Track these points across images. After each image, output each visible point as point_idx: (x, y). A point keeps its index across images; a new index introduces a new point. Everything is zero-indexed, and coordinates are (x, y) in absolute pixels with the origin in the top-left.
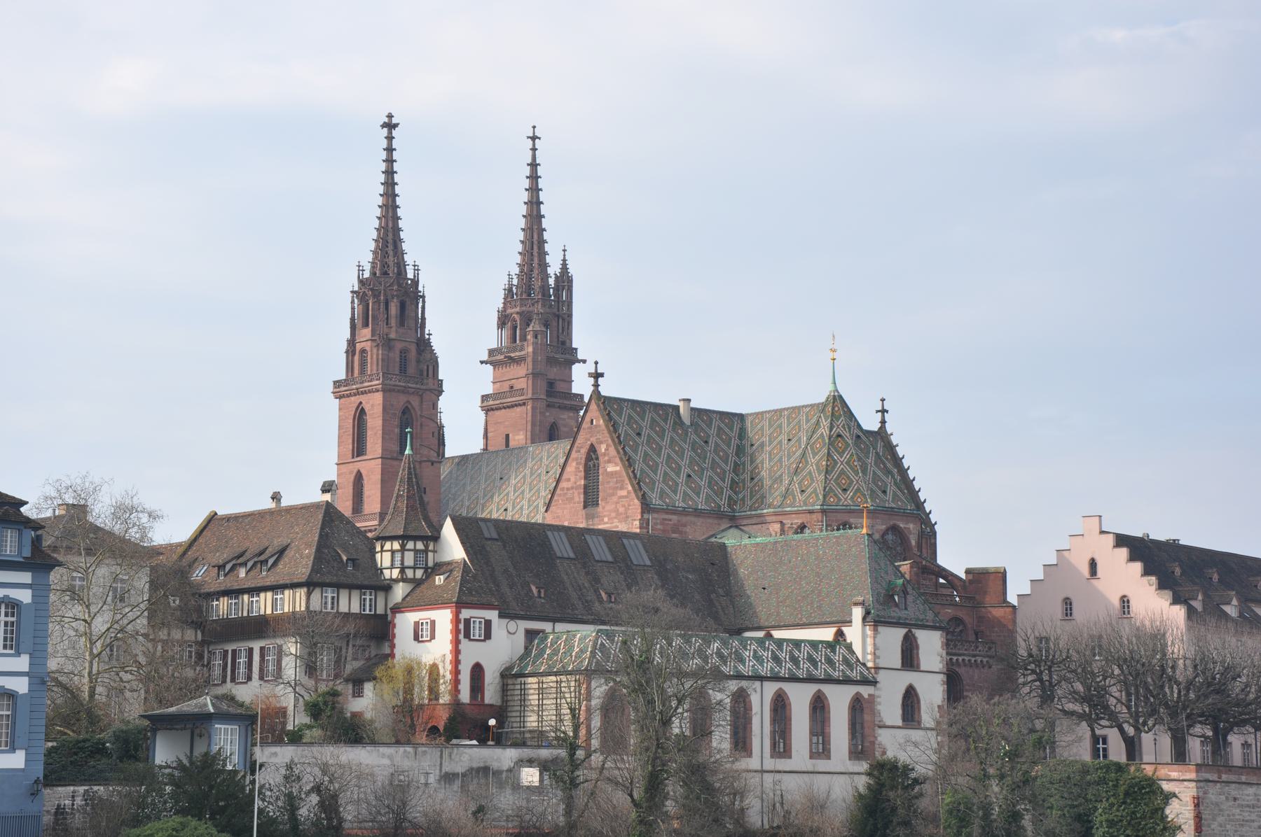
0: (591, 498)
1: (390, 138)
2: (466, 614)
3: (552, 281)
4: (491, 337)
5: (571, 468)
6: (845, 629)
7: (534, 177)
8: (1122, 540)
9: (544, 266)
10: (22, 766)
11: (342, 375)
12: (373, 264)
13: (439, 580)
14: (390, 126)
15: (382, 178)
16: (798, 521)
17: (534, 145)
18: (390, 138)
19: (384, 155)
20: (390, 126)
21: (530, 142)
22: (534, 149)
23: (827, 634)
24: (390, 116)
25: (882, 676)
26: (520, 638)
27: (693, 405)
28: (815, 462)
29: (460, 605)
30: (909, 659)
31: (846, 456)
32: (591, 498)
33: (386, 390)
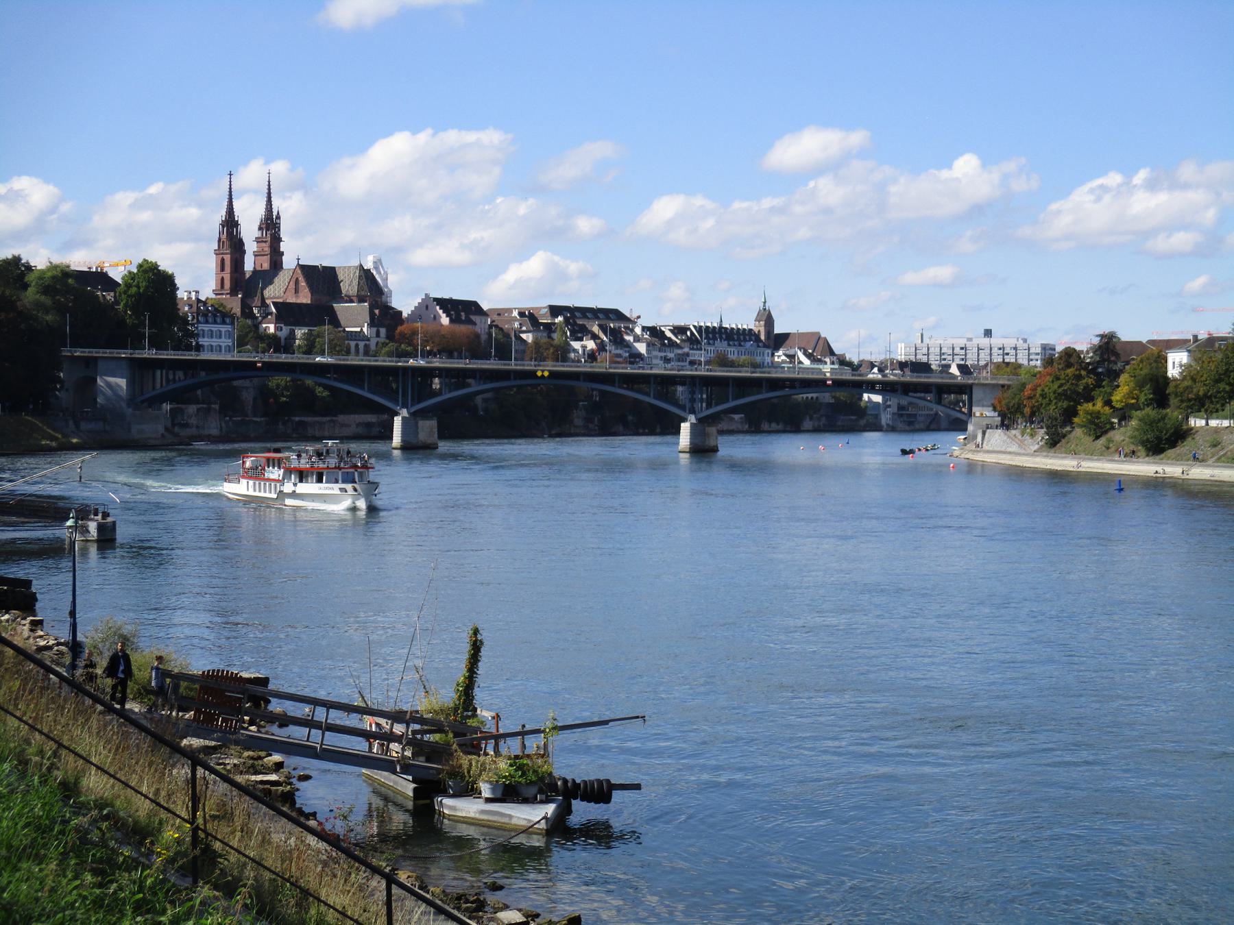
0: (297, 291)
4: (257, 234)
7: (269, 185)
11: (217, 248)
13: (269, 317)
14: (230, 175)
20: (230, 175)
23: (358, 329)
25: (372, 339)
28: (355, 283)
29: (275, 324)
30: (378, 335)
32: (297, 291)
33: (231, 254)
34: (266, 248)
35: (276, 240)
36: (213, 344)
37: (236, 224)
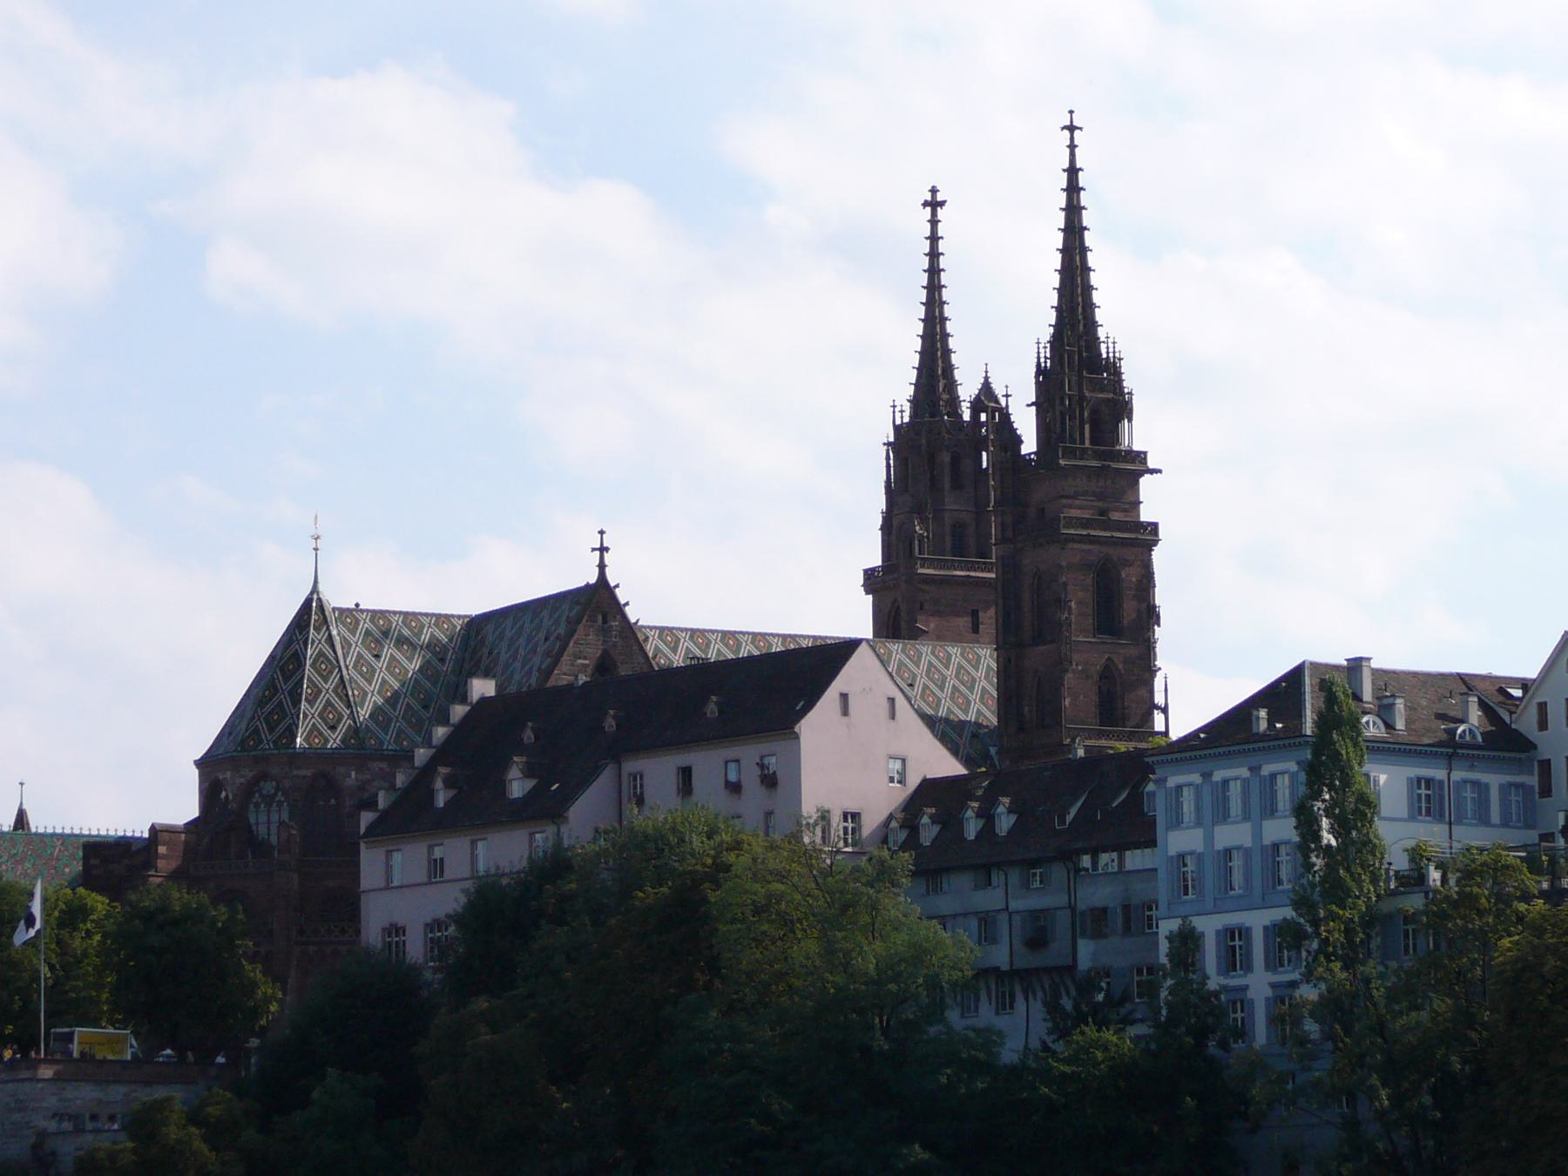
1: (934, 222)
7: (1073, 189)
14: (934, 204)
17: (1072, 139)
18: (934, 222)
20: (934, 204)
21: (1067, 132)
22: (1072, 147)
24: (934, 191)
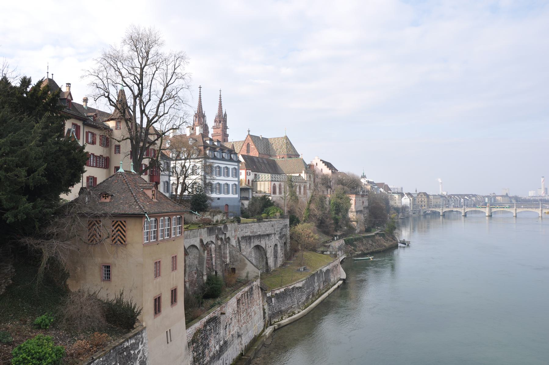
1: (200, 90)
2: (247, 171)
3: (223, 115)
5: (244, 146)
6: (301, 174)
7: (220, 97)
8: (321, 160)
9: (222, 112)
10: (237, 197)
12: (198, 111)
14: (200, 88)
15: (199, 96)
16: (282, 156)
18: (200, 90)
19: (199, 92)
20: (200, 88)
23: (298, 175)
26: (254, 175)
27: (262, 137)
28: (284, 147)
29: (247, 169)
31: (289, 146)
32: (248, 151)
34: (219, 131)
35: (225, 128)
36: (222, 182)
37: (204, 116)
